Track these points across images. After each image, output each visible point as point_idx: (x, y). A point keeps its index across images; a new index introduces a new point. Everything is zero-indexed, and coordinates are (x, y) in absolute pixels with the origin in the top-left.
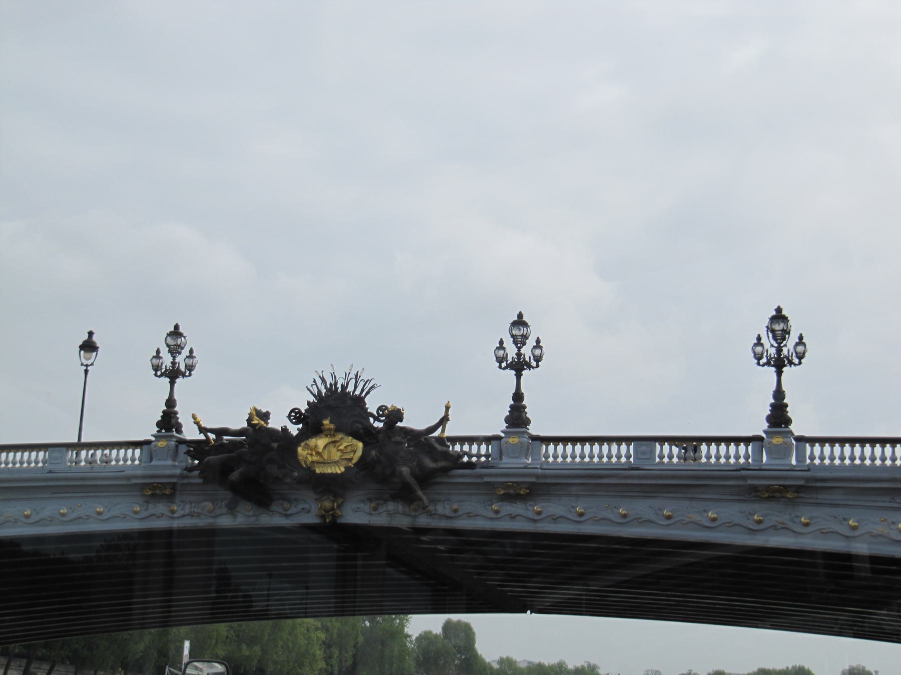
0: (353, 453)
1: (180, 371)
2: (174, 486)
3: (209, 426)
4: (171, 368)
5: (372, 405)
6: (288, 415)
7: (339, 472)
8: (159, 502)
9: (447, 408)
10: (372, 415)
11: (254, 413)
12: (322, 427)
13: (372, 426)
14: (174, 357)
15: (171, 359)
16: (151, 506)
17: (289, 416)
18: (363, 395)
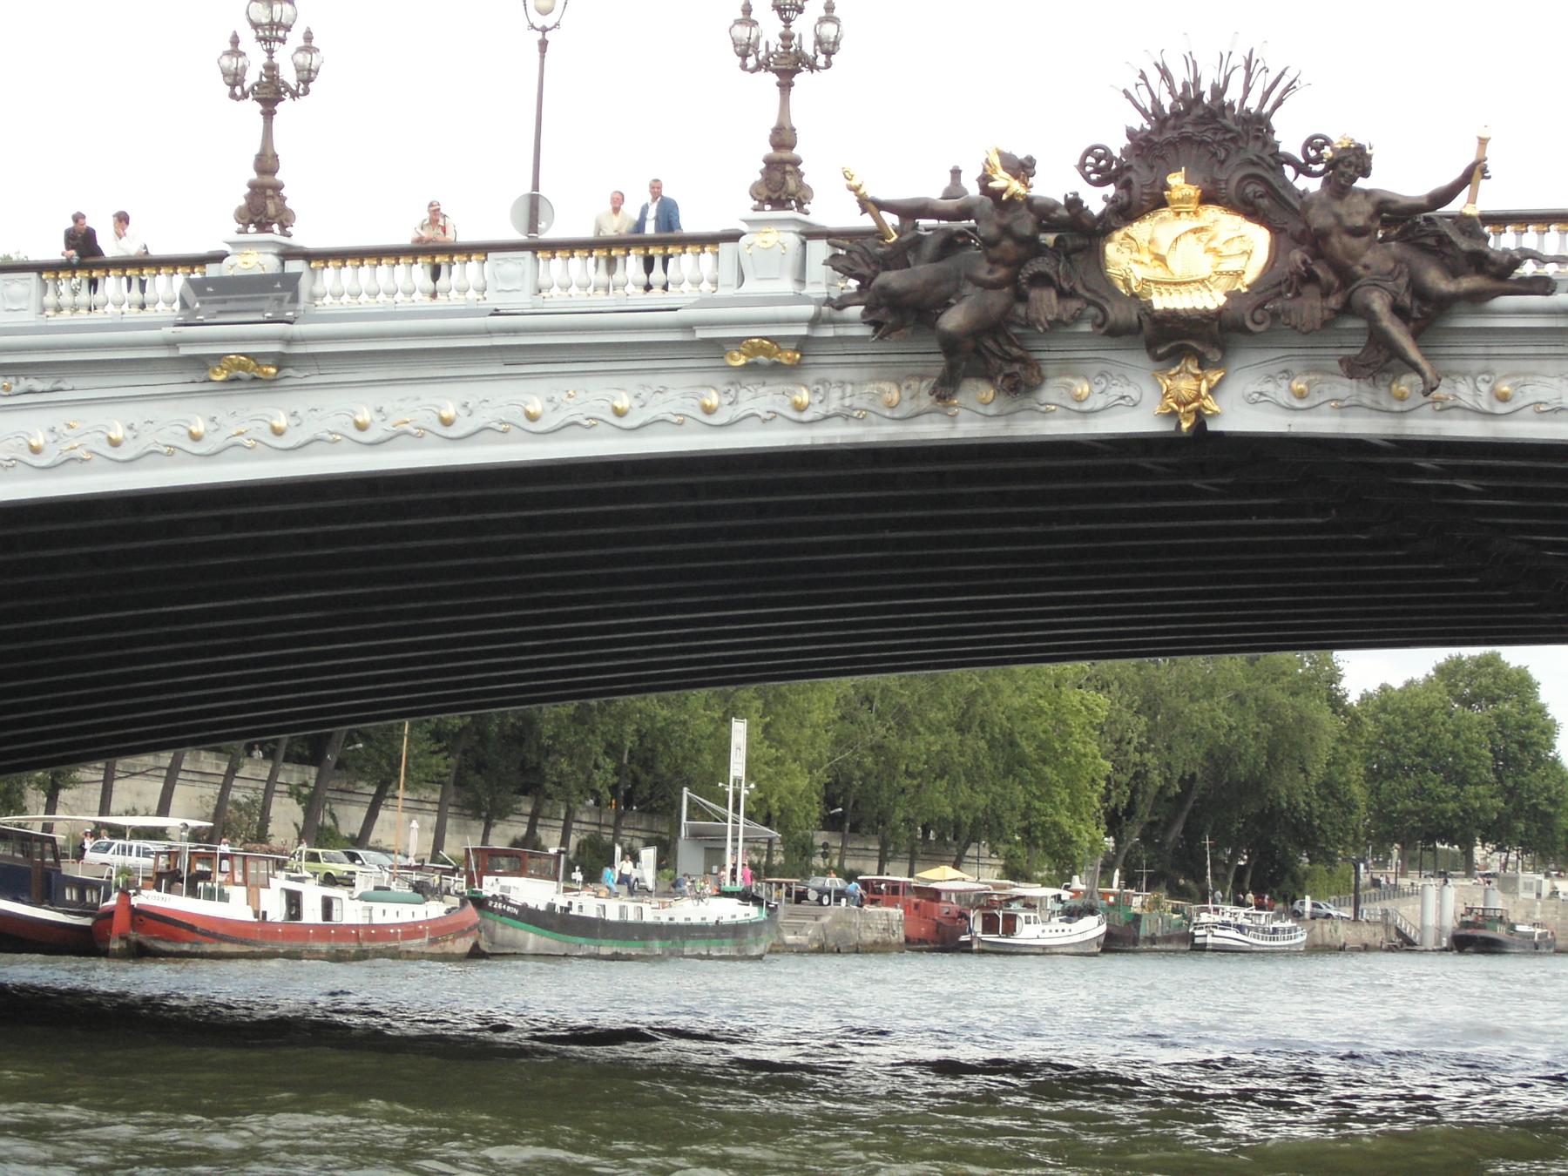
0: (1246, 257)
1: (805, 56)
2: (803, 344)
3: (883, 195)
4: (781, 50)
5: (1289, 136)
6: (1077, 163)
7: (1212, 306)
8: (764, 384)
9: (1483, 142)
10: (1291, 160)
11: (996, 161)
12: (1166, 193)
13: (1288, 186)
14: (788, 21)
15: (779, 26)
16: (744, 395)
17: (1082, 165)
18: (1267, 109)
